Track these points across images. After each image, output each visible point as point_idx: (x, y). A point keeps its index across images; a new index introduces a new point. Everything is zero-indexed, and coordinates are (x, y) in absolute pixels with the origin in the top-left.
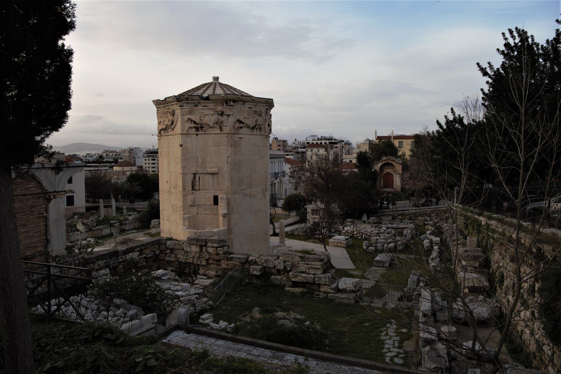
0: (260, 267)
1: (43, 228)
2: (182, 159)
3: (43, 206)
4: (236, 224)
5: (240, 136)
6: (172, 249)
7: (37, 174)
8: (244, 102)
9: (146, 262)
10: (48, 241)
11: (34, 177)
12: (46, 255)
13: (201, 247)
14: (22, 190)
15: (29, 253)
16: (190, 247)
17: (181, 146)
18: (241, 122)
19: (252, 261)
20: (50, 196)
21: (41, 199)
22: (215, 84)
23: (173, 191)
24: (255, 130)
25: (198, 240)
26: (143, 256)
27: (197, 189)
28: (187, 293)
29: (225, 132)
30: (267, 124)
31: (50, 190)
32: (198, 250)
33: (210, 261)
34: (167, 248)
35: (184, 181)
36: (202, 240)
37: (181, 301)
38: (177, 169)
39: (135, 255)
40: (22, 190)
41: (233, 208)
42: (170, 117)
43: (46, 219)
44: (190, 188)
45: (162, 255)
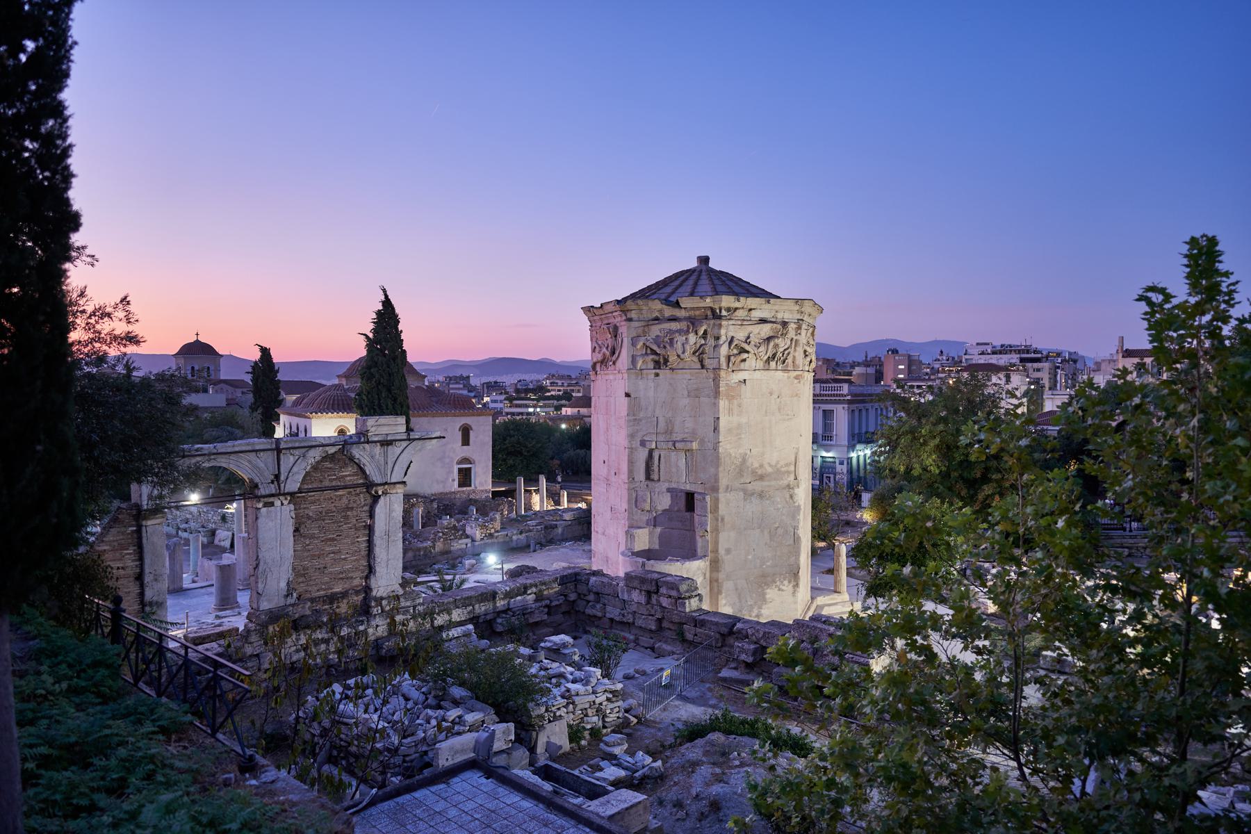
0: (752, 647)
1: (365, 545)
2: (629, 421)
4: (728, 551)
6: (597, 594)
7: (356, 452)
9: (549, 614)
10: (371, 570)
11: (352, 459)
12: (367, 589)
13: (649, 593)
14: (331, 480)
16: (629, 592)
17: (627, 395)
19: (739, 631)
22: (701, 271)
23: (613, 479)
24: (773, 364)
25: (643, 581)
26: (544, 603)
27: (656, 477)
28: (589, 688)
30: (800, 350)
31: (377, 478)
32: (643, 599)
33: (665, 624)
34: (590, 591)
35: (631, 463)
36: (652, 580)
37: (573, 703)
38: (620, 437)
40: (331, 480)
42: (610, 342)
43: (370, 529)
44: (641, 475)
45: (581, 604)
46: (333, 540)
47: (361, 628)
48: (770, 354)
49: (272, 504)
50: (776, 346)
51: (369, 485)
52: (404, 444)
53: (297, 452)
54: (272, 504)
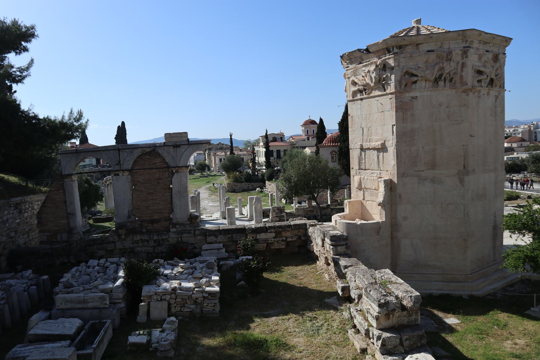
3: (169, 179)
4: (405, 218)
5: (412, 94)
7: (160, 151)
8: (418, 45)
11: (159, 155)
14: (149, 165)
15: (156, 217)
18: (413, 75)
20: (172, 171)
21: (167, 173)
24: (441, 83)
29: (388, 91)
31: (172, 164)
39: (270, 236)
40: (149, 165)
41: (400, 196)
46: (152, 193)
47: (164, 237)
48: (436, 74)
49: (118, 175)
50: (442, 69)
51: (169, 167)
52: (187, 146)
53: (128, 151)
54: (118, 175)
